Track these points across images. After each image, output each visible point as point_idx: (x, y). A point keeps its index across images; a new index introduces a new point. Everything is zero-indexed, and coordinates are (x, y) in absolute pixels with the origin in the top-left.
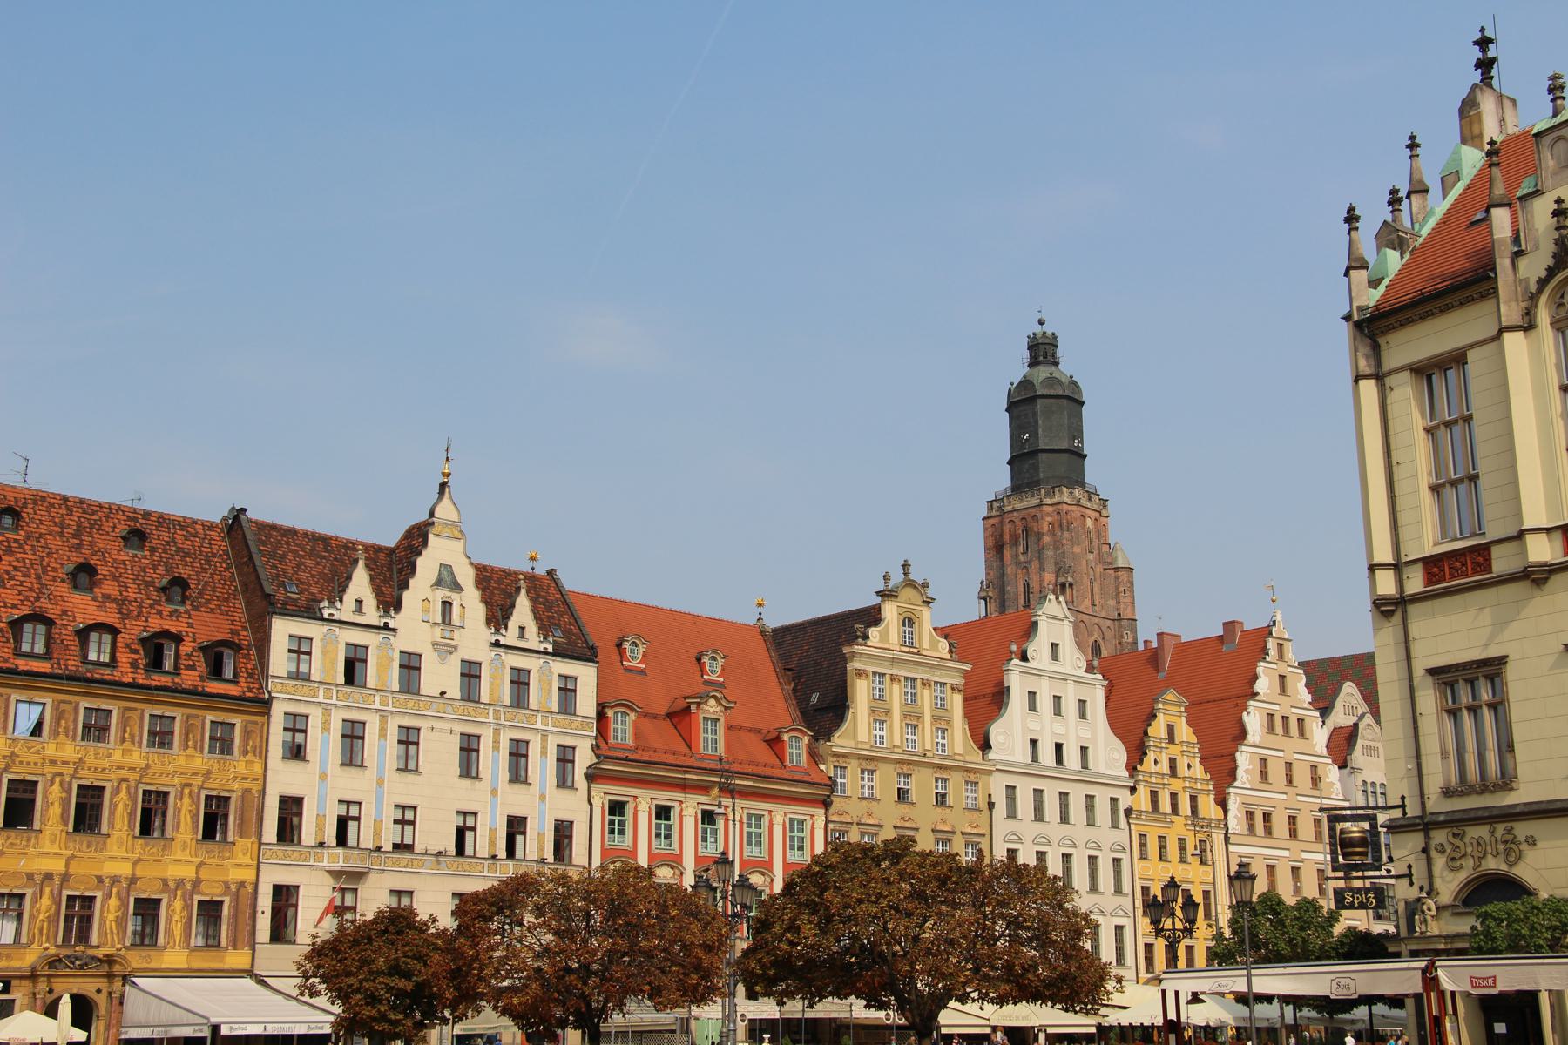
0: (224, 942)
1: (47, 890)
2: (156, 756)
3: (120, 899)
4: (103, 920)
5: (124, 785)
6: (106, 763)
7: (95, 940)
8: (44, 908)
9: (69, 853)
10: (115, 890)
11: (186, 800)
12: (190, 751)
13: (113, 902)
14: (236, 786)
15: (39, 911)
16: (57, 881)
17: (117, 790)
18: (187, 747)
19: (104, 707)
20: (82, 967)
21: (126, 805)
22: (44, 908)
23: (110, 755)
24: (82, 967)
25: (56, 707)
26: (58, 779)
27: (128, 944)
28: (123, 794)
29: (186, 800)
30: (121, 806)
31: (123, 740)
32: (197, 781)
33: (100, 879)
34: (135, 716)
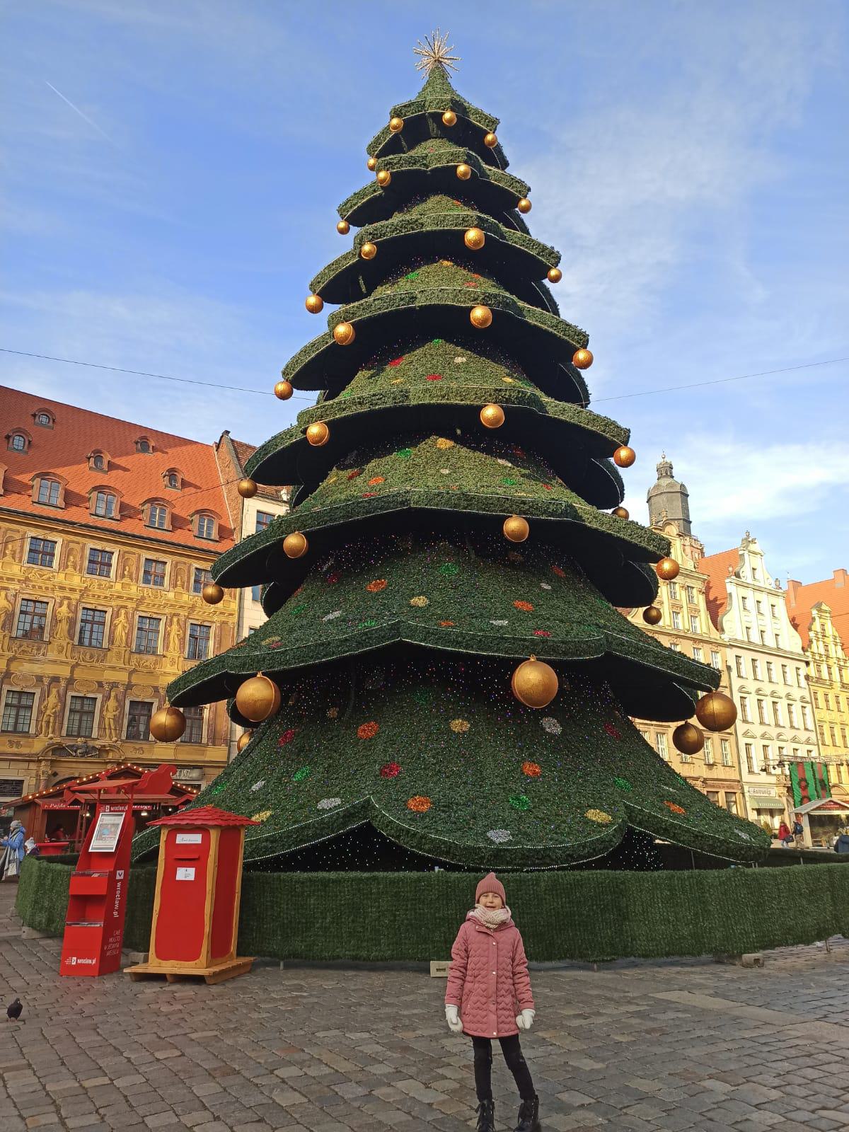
0: (204, 740)
1: (54, 691)
2: (148, 590)
3: (117, 701)
4: (102, 718)
5: (123, 611)
6: (108, 593)
7: (95, 735)
8: (50, 705)
9: (74, 662)
10: (113, 694)
11: (175, 627)
12: (179, 589)
13: (112, 704)
14: (215, 618)
15: (46, 707)
16: (63, 684)
17: (116, 615)
18: (175, 586)
19: (107, 549)
20: (83, 755)
21: (124, 627)
22: (50, 705)
23: (111, 587)
24: (83, 755)
25: (66, 545)
26: (66, 602)
27: (124, 738)
28: (122, 618)
29: (175, 627)
30: (120, 627)
31: (123, 576)
32: (183, 613)
33: (100, 684)
34: (133, 558)
